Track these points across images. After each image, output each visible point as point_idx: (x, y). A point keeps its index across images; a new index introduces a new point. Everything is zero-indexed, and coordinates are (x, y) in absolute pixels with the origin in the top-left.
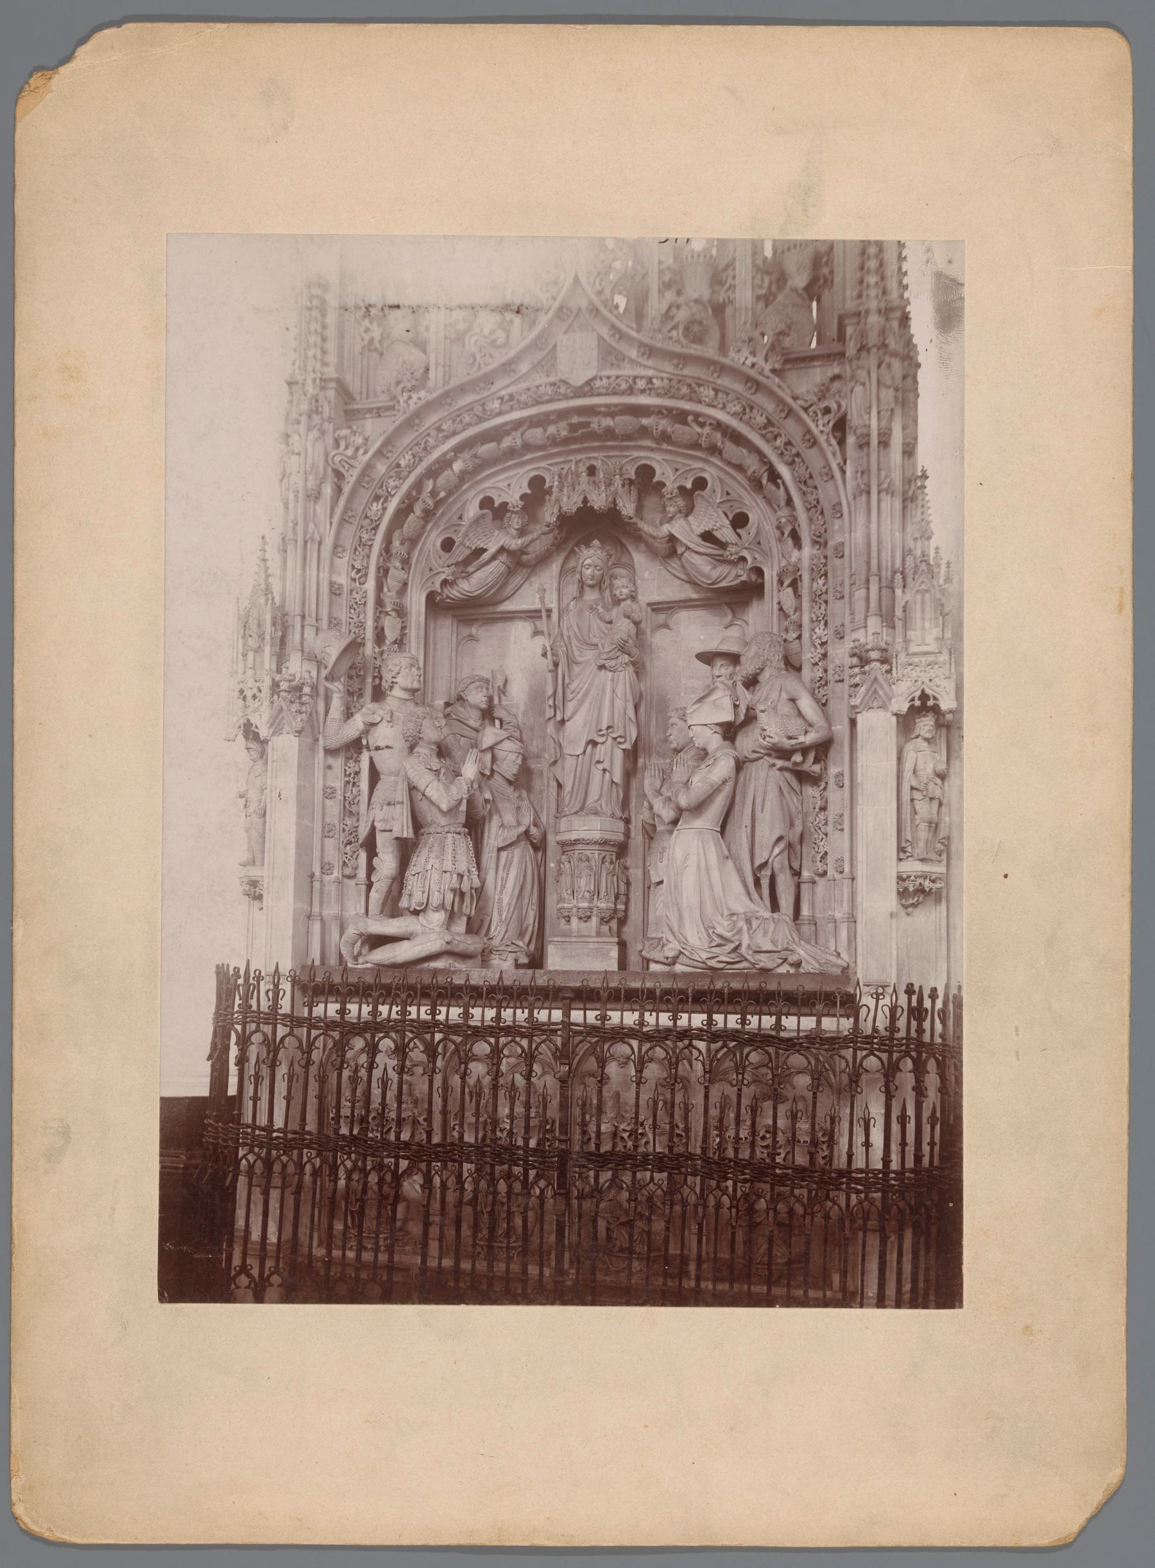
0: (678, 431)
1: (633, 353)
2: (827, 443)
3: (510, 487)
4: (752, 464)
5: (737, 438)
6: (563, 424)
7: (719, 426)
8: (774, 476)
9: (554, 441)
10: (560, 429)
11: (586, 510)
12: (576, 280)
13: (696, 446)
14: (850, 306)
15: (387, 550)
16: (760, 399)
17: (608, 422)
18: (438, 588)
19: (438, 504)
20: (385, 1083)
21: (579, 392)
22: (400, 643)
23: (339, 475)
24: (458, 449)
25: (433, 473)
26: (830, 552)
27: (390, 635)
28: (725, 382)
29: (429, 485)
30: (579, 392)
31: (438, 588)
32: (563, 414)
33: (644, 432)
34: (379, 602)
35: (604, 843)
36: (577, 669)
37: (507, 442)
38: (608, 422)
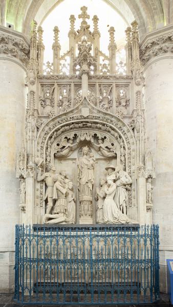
0: (103, 128)
1: (96, 112)
2: (131, 131)
3: (71, 135)
4: (116, 135)
5: (113, 129)
6: (82, 124)
7: (111, 127)
8: (120, 137)
9: (80, 127)
10: (81, 125)
11: (85, 140)
12: (85, 98)
13: (106, 130)
14: (135, 109)
15: (47, 144)
16: (119, 123)
17: (90, 124)
18: (56, 152)
19: (57, 137)
20: (48, 248)
21: (85, 118)
22: (50, 162)
23: (38, 128)
24: (62, 127)
25: (56, 131)
26: (131, 150)
27: (48, 160)
28: (113, 119)
29: (55, 133)
30: (85, 118)
31: (56, 152)
32: (82, 122)
33: (97, 128)
34: (46, 154)
35: (90, 201)
36: (83, 169)
37: (71, 126)
38: (90, 124)
